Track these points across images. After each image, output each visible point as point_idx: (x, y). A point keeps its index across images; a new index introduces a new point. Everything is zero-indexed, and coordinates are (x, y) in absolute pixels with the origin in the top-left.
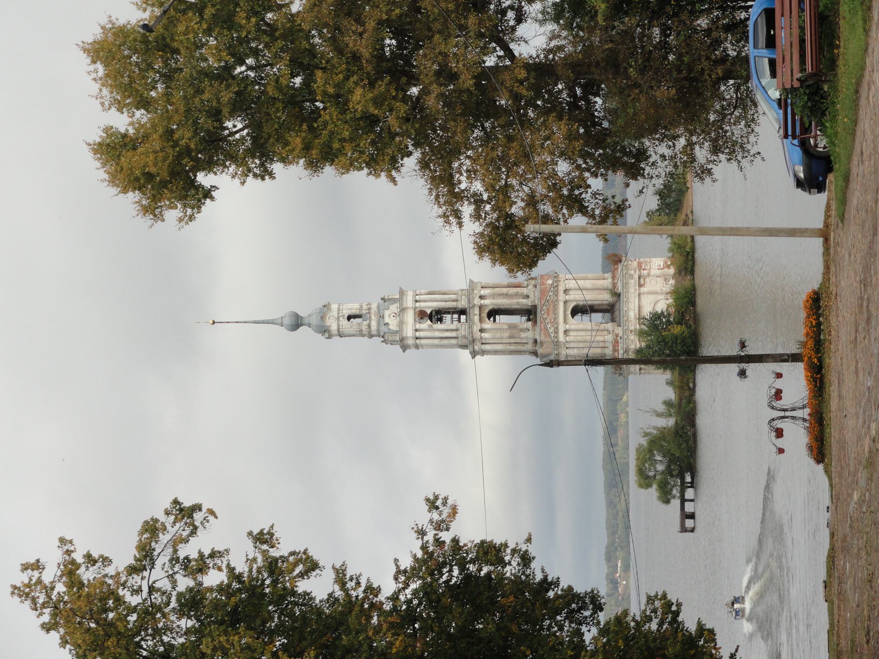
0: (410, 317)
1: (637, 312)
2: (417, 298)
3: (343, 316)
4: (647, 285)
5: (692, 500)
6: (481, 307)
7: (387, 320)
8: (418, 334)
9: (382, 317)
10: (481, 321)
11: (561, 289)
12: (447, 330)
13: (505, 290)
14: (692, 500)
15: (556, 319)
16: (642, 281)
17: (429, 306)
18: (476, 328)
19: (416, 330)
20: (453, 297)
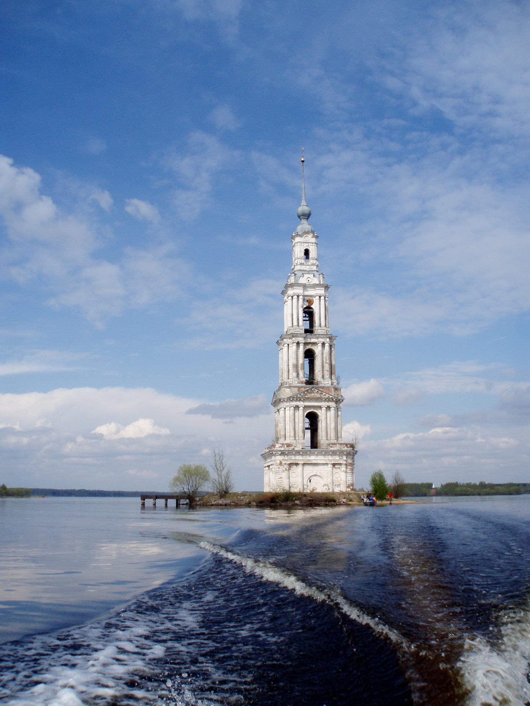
0: (310, 292)
1: (314, 462)
2: (322, 298)
3: (308, 246)
4: (335, 470)
5: (166, 505)
7: (306, 276)
8: (295, 297)
9: (308, 273)
11: (332, 404)
12: (298, 319)
14: (166, 505)
15: (309, 399)
16: (336, 466)
18: (301, 340)
19: (298, 296)
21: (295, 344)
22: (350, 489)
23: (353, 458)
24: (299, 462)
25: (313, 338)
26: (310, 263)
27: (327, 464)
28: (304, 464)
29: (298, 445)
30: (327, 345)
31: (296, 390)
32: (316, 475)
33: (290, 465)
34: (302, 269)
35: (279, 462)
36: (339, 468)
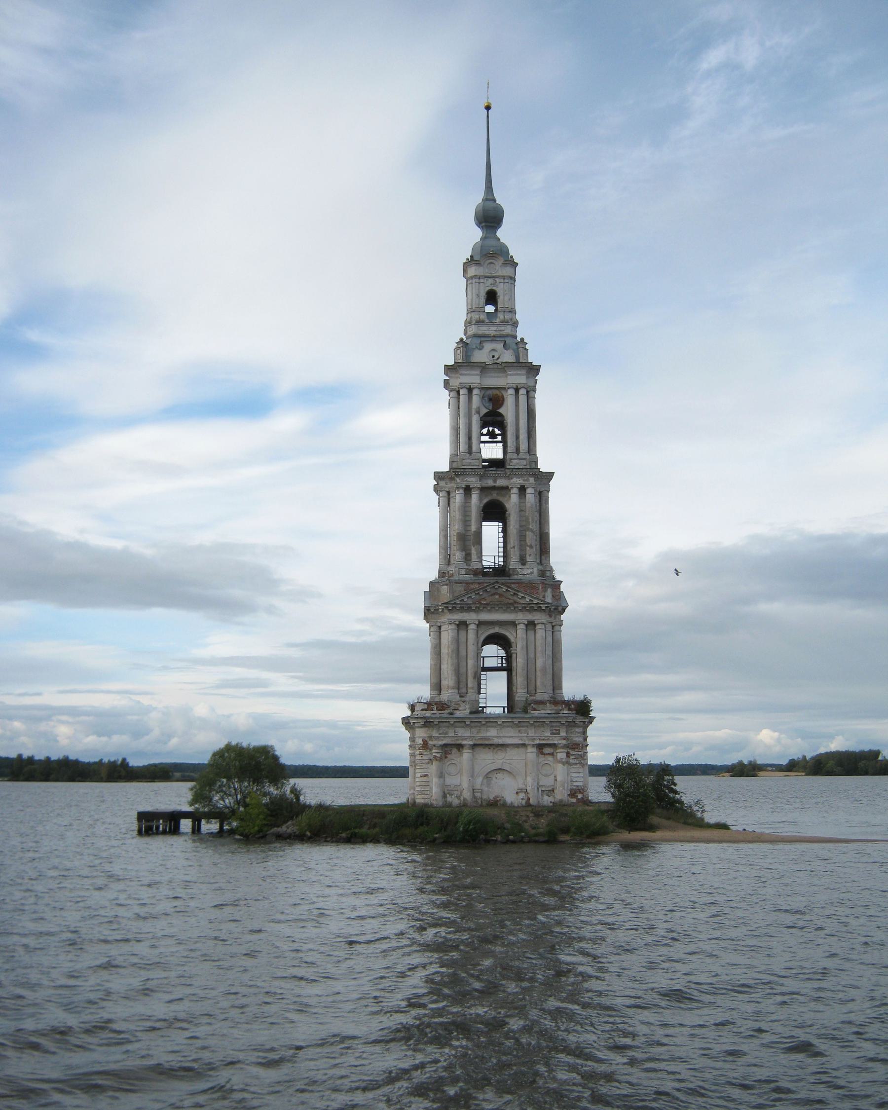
0: (494, 381)
2: (522, 392)
3: (494, 284)
4: (542, 759)
6: (506, 489)
7: (488, 346)
10: (483, 490)
11: (537, 617)
13: (534, 526)
16: (547, 750)
17: (508, 411)
18: (473, 481)
19: (470, 390)
20: (524, 446)
21: (461, 491)
22: (574, 800)
23: (584, 733)
24: (464, 742)
25: (500, 477)
26: (498, 320)
27: (524, 745)
28: (474, 746)
29: (462, 705)
30: (529, 491)
31: (460, 589)
32: (500, 770)
33: (446, 749)
34: (480, 332)
35: (420, 741)
36: (552, 754)
